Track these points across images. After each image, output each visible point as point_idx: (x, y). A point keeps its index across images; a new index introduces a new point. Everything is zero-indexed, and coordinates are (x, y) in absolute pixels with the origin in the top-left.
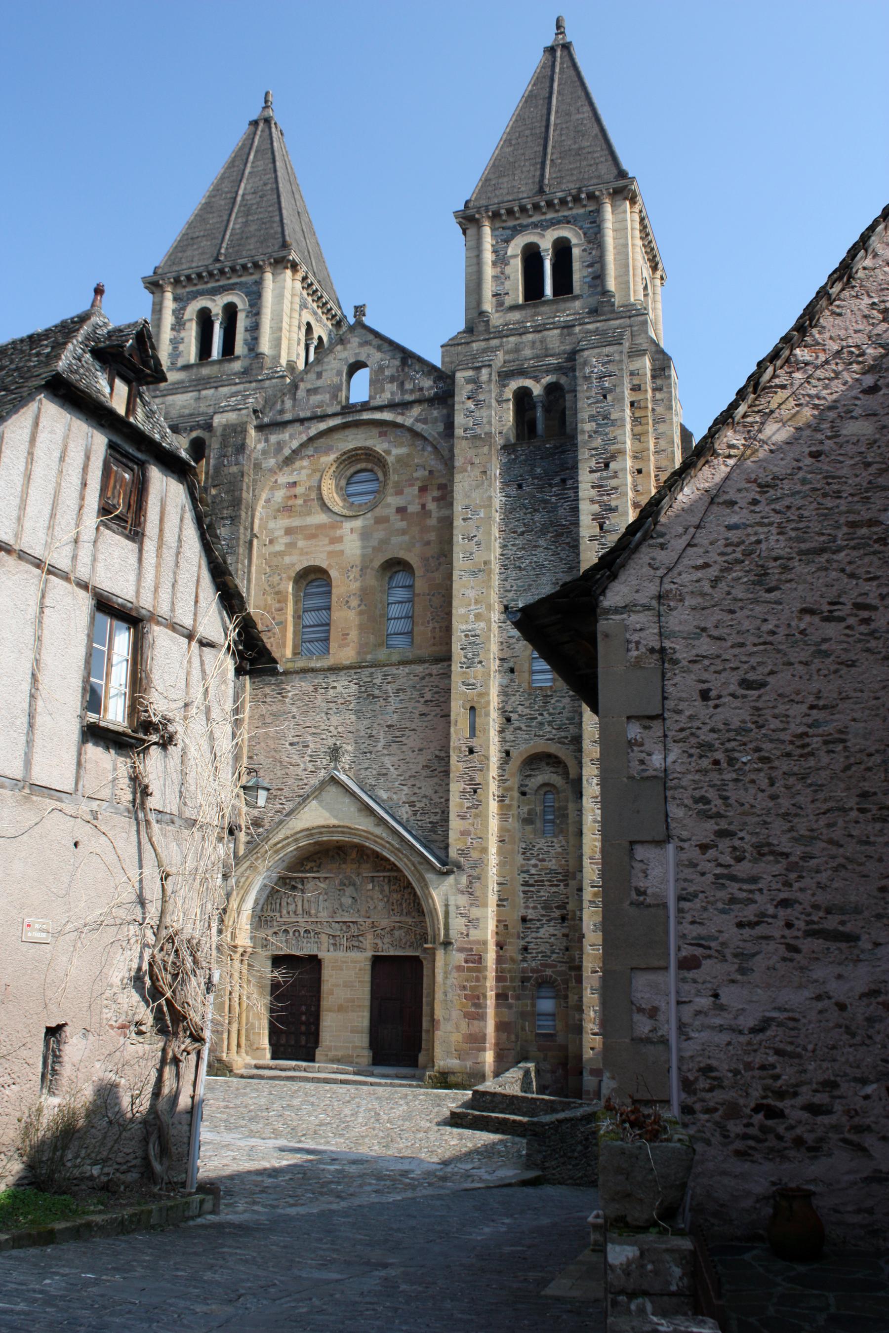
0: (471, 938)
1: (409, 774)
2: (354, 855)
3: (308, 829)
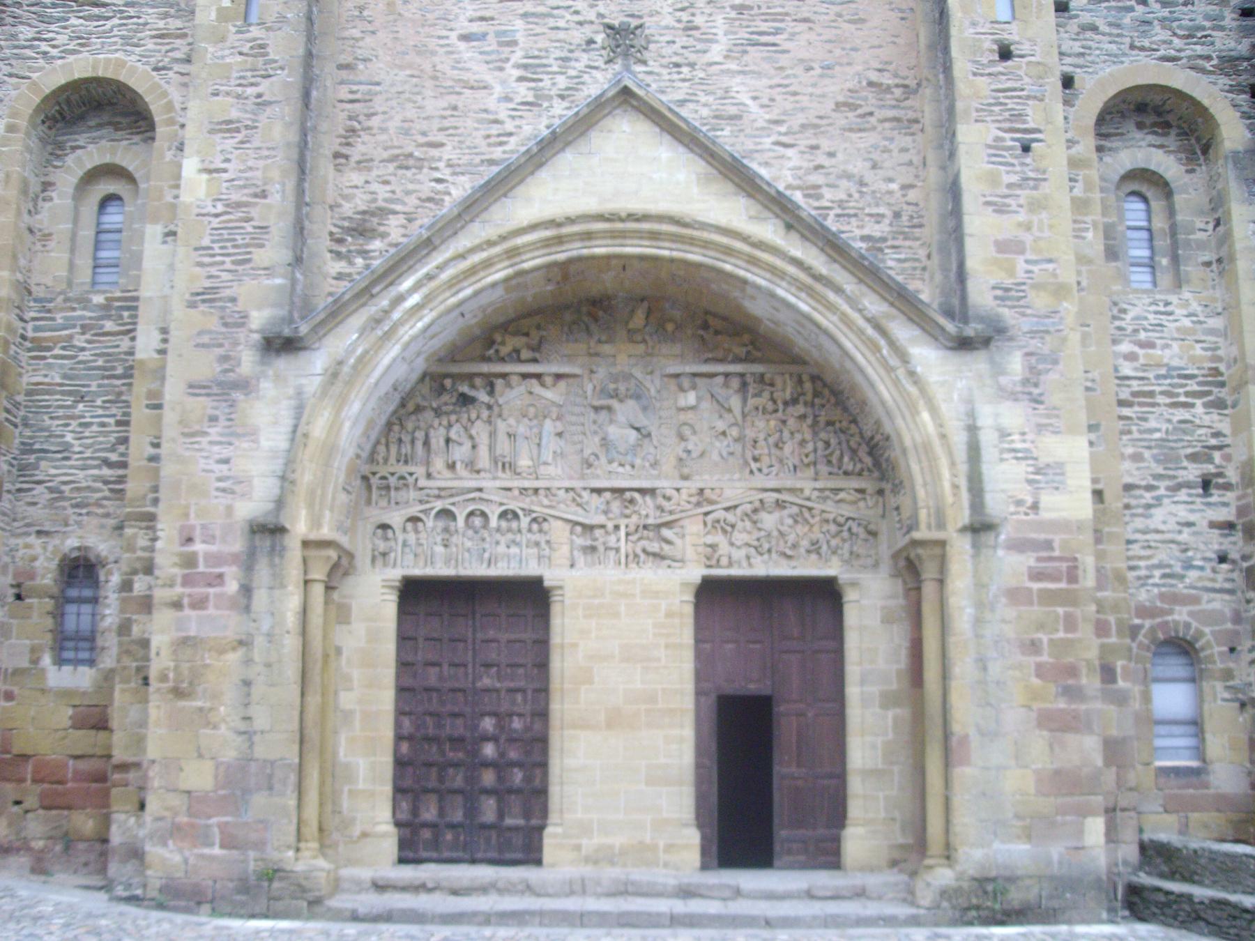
0: (1045, 515)
1: (800, 119)
2: (639, 319)
3: (552, 223)
